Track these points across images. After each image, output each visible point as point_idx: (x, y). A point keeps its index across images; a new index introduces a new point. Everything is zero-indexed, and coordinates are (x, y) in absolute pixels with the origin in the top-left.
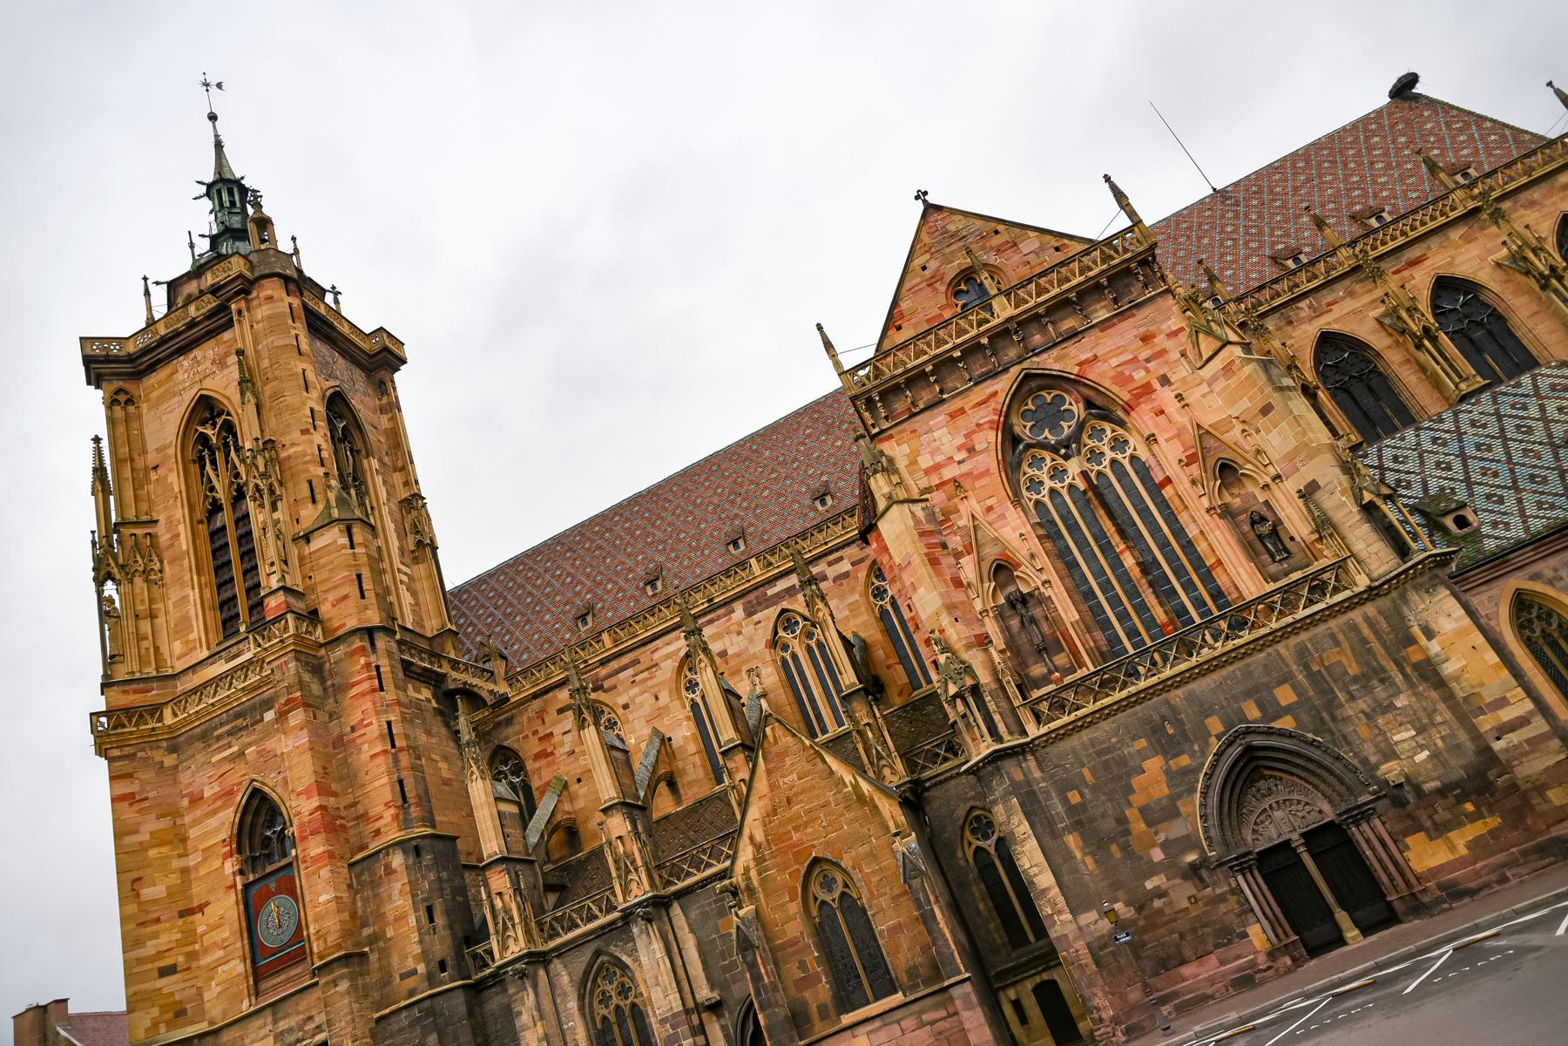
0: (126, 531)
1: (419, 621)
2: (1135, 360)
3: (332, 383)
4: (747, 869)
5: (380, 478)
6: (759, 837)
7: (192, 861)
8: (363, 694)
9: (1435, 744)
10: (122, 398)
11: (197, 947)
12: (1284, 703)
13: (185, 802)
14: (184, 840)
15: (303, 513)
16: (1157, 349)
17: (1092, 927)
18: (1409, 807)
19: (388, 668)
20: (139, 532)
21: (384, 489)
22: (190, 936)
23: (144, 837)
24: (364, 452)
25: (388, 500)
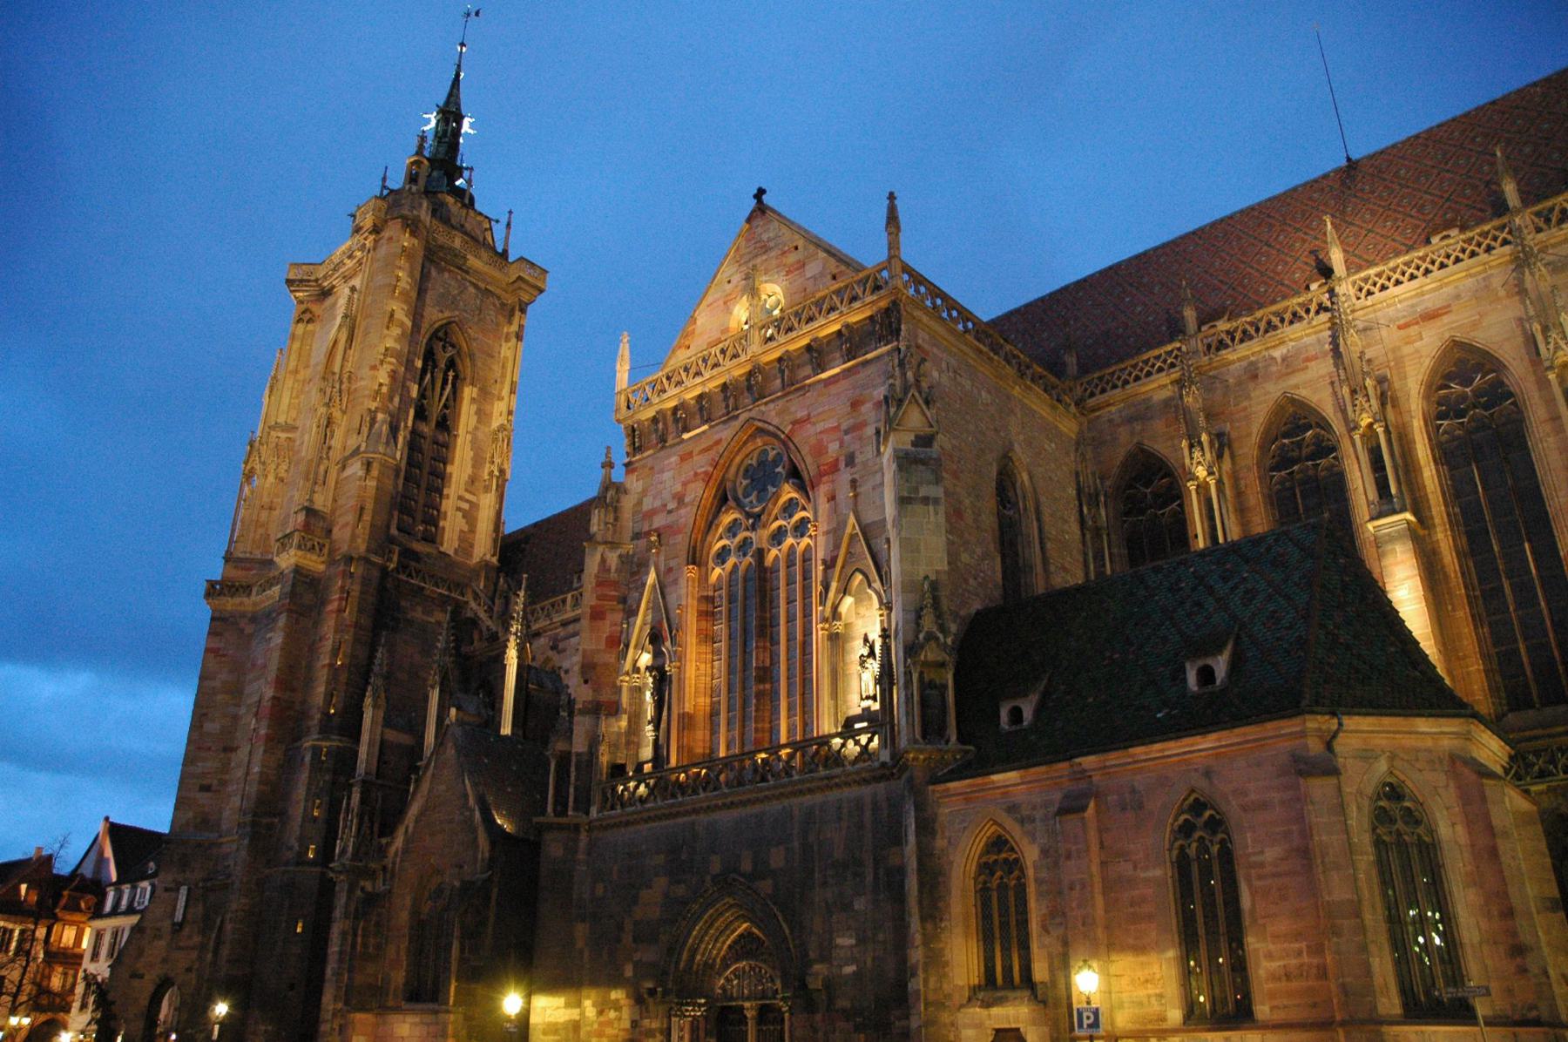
0: (273, 434)
1: (466, 543)
2: (837, 428)
3: (447, 314)
4: (396, 854)
5: (474, 408)
6: (410, 830)
7: (243, 711)
8: (332, 611)
9: (865, 963)
10: (307, 316)
11: (227, 777)
12: (773, 865)
13: (249, 665)
14: (241, 692)
15: (349, 442)
16: (861, 419)
17: (549, 1012)
18: (818, 1017)
19: (357, 594)
20: (283, 435)
21: (473, 420)
22: (225, 768)
23: (217, 684)
24: (468, 381)
25: (476, 428)
